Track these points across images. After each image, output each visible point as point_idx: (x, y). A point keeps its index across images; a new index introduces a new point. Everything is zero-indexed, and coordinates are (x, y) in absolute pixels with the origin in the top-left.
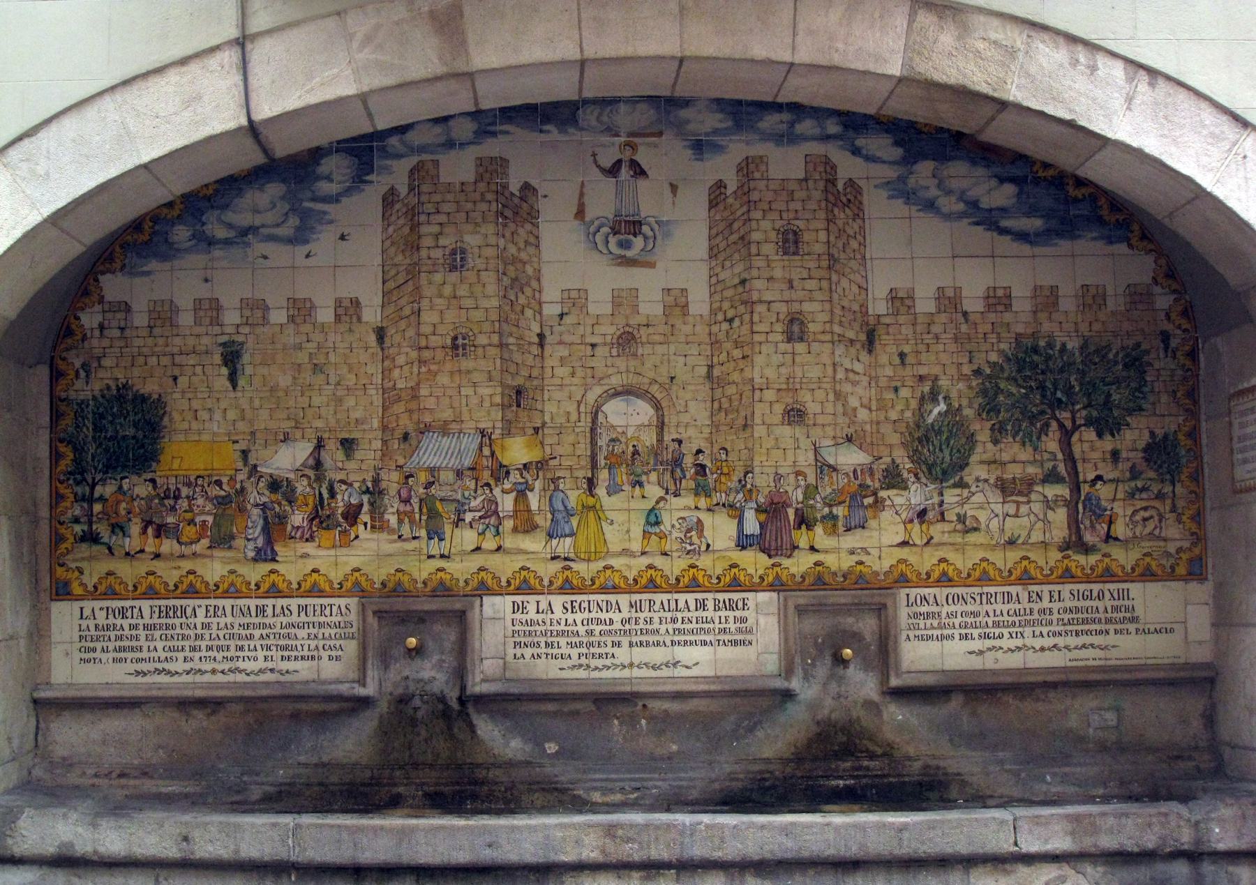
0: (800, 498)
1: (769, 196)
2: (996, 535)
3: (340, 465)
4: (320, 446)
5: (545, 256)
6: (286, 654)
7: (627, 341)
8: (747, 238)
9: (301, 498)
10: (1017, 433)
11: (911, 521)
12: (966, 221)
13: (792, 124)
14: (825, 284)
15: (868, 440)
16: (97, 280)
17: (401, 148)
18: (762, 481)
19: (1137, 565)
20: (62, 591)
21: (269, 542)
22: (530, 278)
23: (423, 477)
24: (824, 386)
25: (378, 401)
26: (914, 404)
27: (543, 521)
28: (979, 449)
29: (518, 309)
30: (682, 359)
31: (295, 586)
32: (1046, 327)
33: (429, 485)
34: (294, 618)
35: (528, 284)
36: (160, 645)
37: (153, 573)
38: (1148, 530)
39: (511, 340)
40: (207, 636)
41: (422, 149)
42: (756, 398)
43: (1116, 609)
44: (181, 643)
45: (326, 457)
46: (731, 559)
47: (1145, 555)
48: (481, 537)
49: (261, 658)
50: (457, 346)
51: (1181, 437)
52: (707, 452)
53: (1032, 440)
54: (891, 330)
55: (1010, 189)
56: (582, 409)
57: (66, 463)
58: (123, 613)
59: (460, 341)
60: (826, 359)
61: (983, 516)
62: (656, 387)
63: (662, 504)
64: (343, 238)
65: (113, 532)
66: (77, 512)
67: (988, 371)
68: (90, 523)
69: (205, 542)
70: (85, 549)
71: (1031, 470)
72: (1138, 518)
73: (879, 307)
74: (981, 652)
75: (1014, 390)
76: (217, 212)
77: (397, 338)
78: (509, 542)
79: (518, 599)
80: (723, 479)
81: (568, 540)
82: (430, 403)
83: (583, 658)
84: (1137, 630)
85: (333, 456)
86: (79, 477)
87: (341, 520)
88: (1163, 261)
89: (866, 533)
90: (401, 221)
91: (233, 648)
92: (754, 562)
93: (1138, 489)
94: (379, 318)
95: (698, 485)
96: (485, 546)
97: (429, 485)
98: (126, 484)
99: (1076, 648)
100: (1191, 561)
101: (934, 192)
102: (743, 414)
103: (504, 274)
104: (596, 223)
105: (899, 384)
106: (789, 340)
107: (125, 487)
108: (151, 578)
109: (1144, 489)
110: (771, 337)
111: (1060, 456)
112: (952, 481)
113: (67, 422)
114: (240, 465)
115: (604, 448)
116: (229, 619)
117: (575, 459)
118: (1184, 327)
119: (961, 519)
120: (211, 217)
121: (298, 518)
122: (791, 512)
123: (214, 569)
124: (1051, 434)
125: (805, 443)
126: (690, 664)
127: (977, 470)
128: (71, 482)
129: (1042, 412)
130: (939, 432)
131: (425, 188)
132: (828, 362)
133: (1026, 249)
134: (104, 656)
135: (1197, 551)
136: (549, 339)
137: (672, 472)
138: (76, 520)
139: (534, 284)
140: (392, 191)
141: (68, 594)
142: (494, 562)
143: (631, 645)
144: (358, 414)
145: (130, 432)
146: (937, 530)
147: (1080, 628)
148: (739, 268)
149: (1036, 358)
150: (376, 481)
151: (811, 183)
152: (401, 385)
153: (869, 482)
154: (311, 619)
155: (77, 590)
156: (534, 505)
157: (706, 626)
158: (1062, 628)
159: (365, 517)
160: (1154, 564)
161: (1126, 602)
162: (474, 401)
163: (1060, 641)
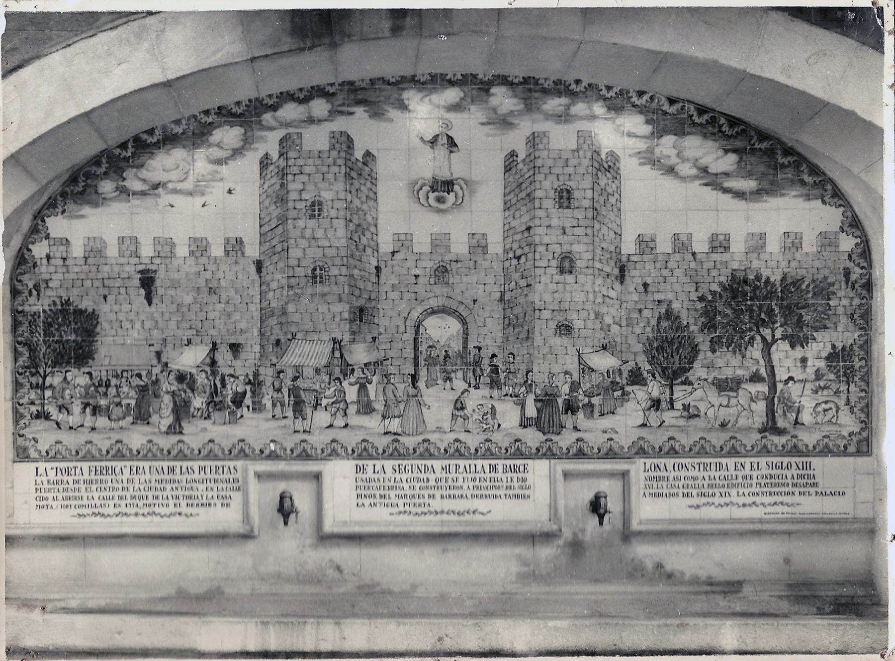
0: (567, 392)
1: (550, 163)
2: (712, 421)
3: (230, 363)
4: (214, 347)
5: (382, 208)
6: (190, 502)
7: (442, 272)
8: (532, 196)
9: (200, 387)
10: (730, 345)
11: (649, 409)
12: (698, 182)
13: (568, 107)
14: (589, 231)
15: (619, 349)
16: (43, 221)
17: (273, 123)
18: (539, 377)
19: (818, 444)
20: (22, 455)
21: (178, 420)
22: (370, 224)
23: (290, 373)
24: (586, 307)
25: (257, 315)
26: (654, 322)
27: (379, 406)
28: (701, 356)
29: (361, 247)
30: (481, 287)
31: (196, 452)
32: (756, 264)
33: (295, 379)
34: (196, 476)
35: (368, 229)
36: (96, 495)
37: (91, 442)
38: (827, 419)
39: (356, 272)
40: (131, 489)
41: (287, 125)
42: (536, 316)
43: (802, 477)
44: (111, 494)
45: (218, 356)
46: (515, 435)
47: (824, 437)
48: (333, 418)
49: (172, 505)
50: (316, 276)
51: (855, 348)
52: (500, 356)
53: (740, 349)
54: (638, 266)
55: (732, 158)
56: (408, 321)
57: (24, 360)
58: (68, 471)
59: (318, 272)
60: (588, 287)
61: (702, 407)
62: (464, 306)
63: (466, 394)
64: (230, 192)
65: (60, 411)
66: (33, 396)
67: (710, 298)
68: (43, 405)
69: (130, 419)
70: (40, 424)
71: (740, 372)
72: (820, 409)
73: (629, 247)
74: (698, 507)
75: (728, 311)
76: (135, 170)
77: (271, 268)
78: (355, 420)
79: (360, 463)
80: (511, 377)
81: (397, 420)
82: (296, 318)
83: (407, 507)
84: (817, 493)
85: (224, 357)
86: (34, 370)
87: (230, 403)
88: (849, 214)
89: (617, 417)
90: (274, 180)
91: (150, 497)
92: (533, 438)
93: (820, 387)
94: (258, 254)
95: (492, 381)
96: (336, 424)
97: (295, 379)
98: (69, 376)
99: (769, 504)
100: (859, 442)
101: (674, 160)
102: (526, 328)
103: (351, 221)
104: (420, 183)
105: (643, 307)
106: (562, 272)
107: (69, 378)
108: (89, 446)
109: (826, 387)
110: (548, 270)
111: (762, 362)
112: (680, 380)
113: (24, 328)
114: (155, 362)
115: (424, 352)
116: (148, 476)
117: (403, 360)
118: (862, 265)
119: (686, 407)
120: (129, 173)
121: (198, 402)
122: (560, 401)
123: (137, 438)
124: (755, 346)
125: (572, 351)
126: (485, 511)
127: (698, 371)
128: (27, 374)
129: (751, 329)
130: (671, 343)
131: (292, 154)
132: (590, 290)
133: (741, 204)
134: (54, 504)
135: (865, 434)
136: (384, 271)
137: (474, 371)
138: (33, 403)
139: (373, 229)
140: (267, 156)
141: (27, 457)
142: (343, 436)
143: (442, 497)
144: (243, 325)
145: (73, 337)
146: (669, 417)
147: (773, 490)
148: (525, 219)
149: (747, 288)
150: (256, 375)
151: (581, 153)
152: (273, 305)
153: (618, 379)
154: (208, 476)
155: (33, 454)
156: (372, 396)
157: (497, 484)
158: (758, 490)
159: (248, 401)
160: (831, 444)
161: (809, 472)
162: (329, 316)
163: (758, 500)
